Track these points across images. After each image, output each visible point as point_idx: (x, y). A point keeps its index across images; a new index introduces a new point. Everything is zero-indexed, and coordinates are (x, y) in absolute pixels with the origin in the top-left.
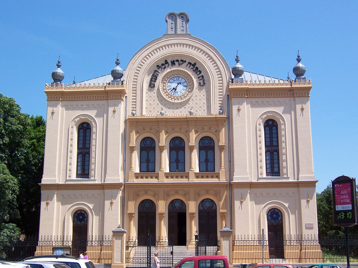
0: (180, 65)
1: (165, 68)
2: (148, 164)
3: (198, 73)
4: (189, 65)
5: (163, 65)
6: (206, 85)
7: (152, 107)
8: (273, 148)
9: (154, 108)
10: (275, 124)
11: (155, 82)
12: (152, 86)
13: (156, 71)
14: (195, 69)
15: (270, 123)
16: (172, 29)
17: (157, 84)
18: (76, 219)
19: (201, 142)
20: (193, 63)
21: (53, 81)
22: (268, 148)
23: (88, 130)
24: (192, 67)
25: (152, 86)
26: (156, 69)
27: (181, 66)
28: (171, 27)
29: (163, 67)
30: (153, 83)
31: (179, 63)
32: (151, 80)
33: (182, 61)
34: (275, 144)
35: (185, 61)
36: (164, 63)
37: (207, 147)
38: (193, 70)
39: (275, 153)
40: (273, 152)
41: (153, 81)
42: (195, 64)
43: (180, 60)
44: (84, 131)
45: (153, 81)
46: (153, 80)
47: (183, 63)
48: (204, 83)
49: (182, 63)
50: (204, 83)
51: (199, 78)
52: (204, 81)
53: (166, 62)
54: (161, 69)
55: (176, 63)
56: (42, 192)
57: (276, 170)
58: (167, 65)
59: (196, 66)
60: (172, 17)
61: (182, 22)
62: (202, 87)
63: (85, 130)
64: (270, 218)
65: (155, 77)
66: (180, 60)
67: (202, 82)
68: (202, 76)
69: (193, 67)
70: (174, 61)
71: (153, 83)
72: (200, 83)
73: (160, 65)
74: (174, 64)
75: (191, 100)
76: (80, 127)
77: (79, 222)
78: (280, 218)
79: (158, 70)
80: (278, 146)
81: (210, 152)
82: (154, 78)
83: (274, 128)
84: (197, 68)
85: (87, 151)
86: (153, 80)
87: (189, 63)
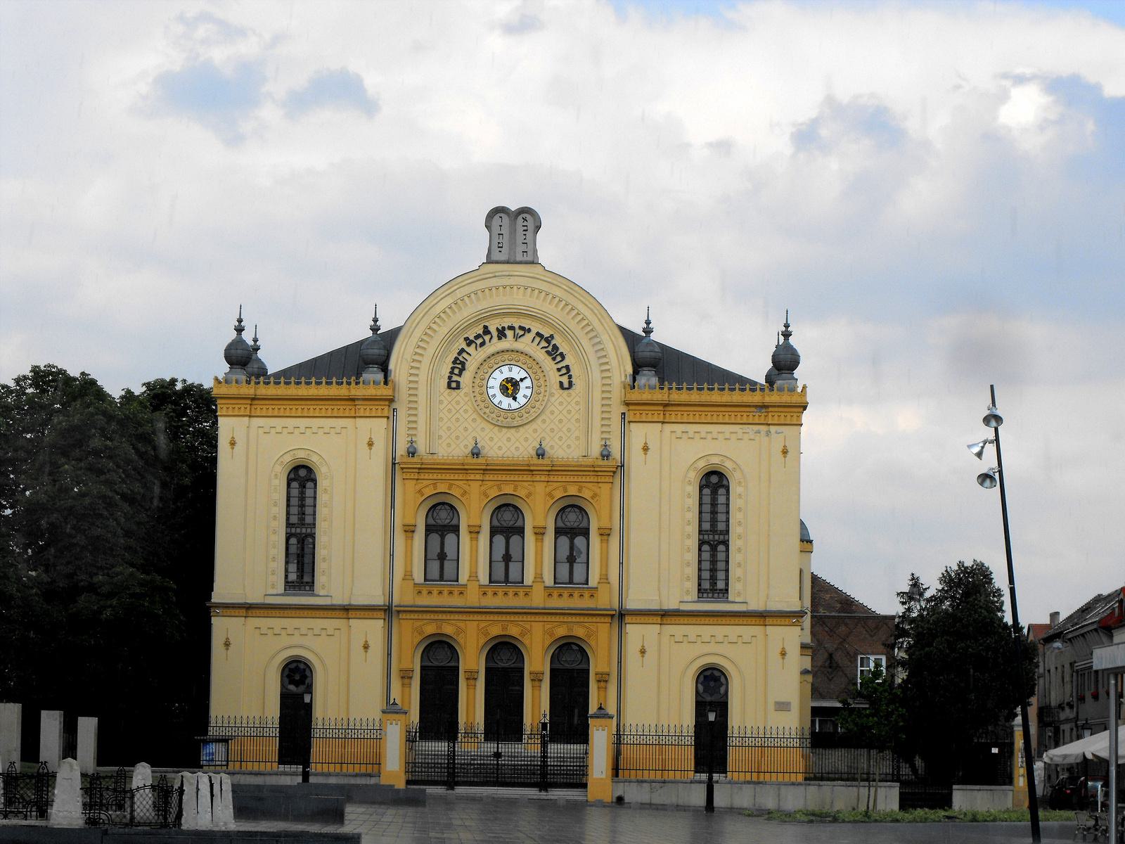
0: (516, 337)
1: (483, 344)
2: (441, 564)
3: (559, 359)
4: (538, 339)
5: (478, 337)
6: (574, 387)
7: (453, 437)
8: (717, 537)
9: (457, 438)
10: (725, 482)
11: (460, 375)
12: (453, 385)
13: (462, 351)
14: (550, 349)
15: (714, 479)
16: (500, 249)
17: (466, 379)
18: (286, 680)
19: (559, 518)
20: (546, 335)
21: (226, 367)
22: (706, 537)
23: (310, 484)
24: (544, 344)
25: (454, 385)
26: (464, 346)
27: (519, 340)
28: (499, 243)
29: (479, 341)
30: (455, 378)
31: (516, 334)
32: (452, 372)
33: (521, 328)
34: (721, 526)
35: (529, 330)
36: (481, 332)
37: (572, 526)
38: (548, 352)
39: (721, 548)
40: (716, 546)
41: (455, 374)
42: (552, 336)
43: (517, 327)
44: (300, 485)
45: (455, 374)
46: (456, 371)
47: (523, 335)
48: (571, 384)
49: (521, 333)
50: (571, 384)
51: (559, 370)
52: (570, 377)
53: (486, 331)
54: (474, 345)
55: (509, 333)
56: (214, 620)
57: (721, 585)
58: (487, 338)
59: (553, 342)
60: (501, 217)
61: (525, 233)
62: (566, 391)
63: (302, 478)
64: (701, 688)
65: (460, 366)
66: (516, 326)
67: (565, 380)
68: (567, 367)
69: (547, 345)
70: (503, 328)
71: (455, 378)
72: (561, 383)
73: (472, 338)
74: (505, 336)
75: (539, 421)
76: (292, 476)
77: (292, 687)
78: (722, 690)
79: (467, 349)
80: (727, 532)
81: (579, 541)
82: (459, 365)
83: (722, 491)
84: (555, 348)
85: (309, 530)
86: (456, 371)
87: (538, 334)
